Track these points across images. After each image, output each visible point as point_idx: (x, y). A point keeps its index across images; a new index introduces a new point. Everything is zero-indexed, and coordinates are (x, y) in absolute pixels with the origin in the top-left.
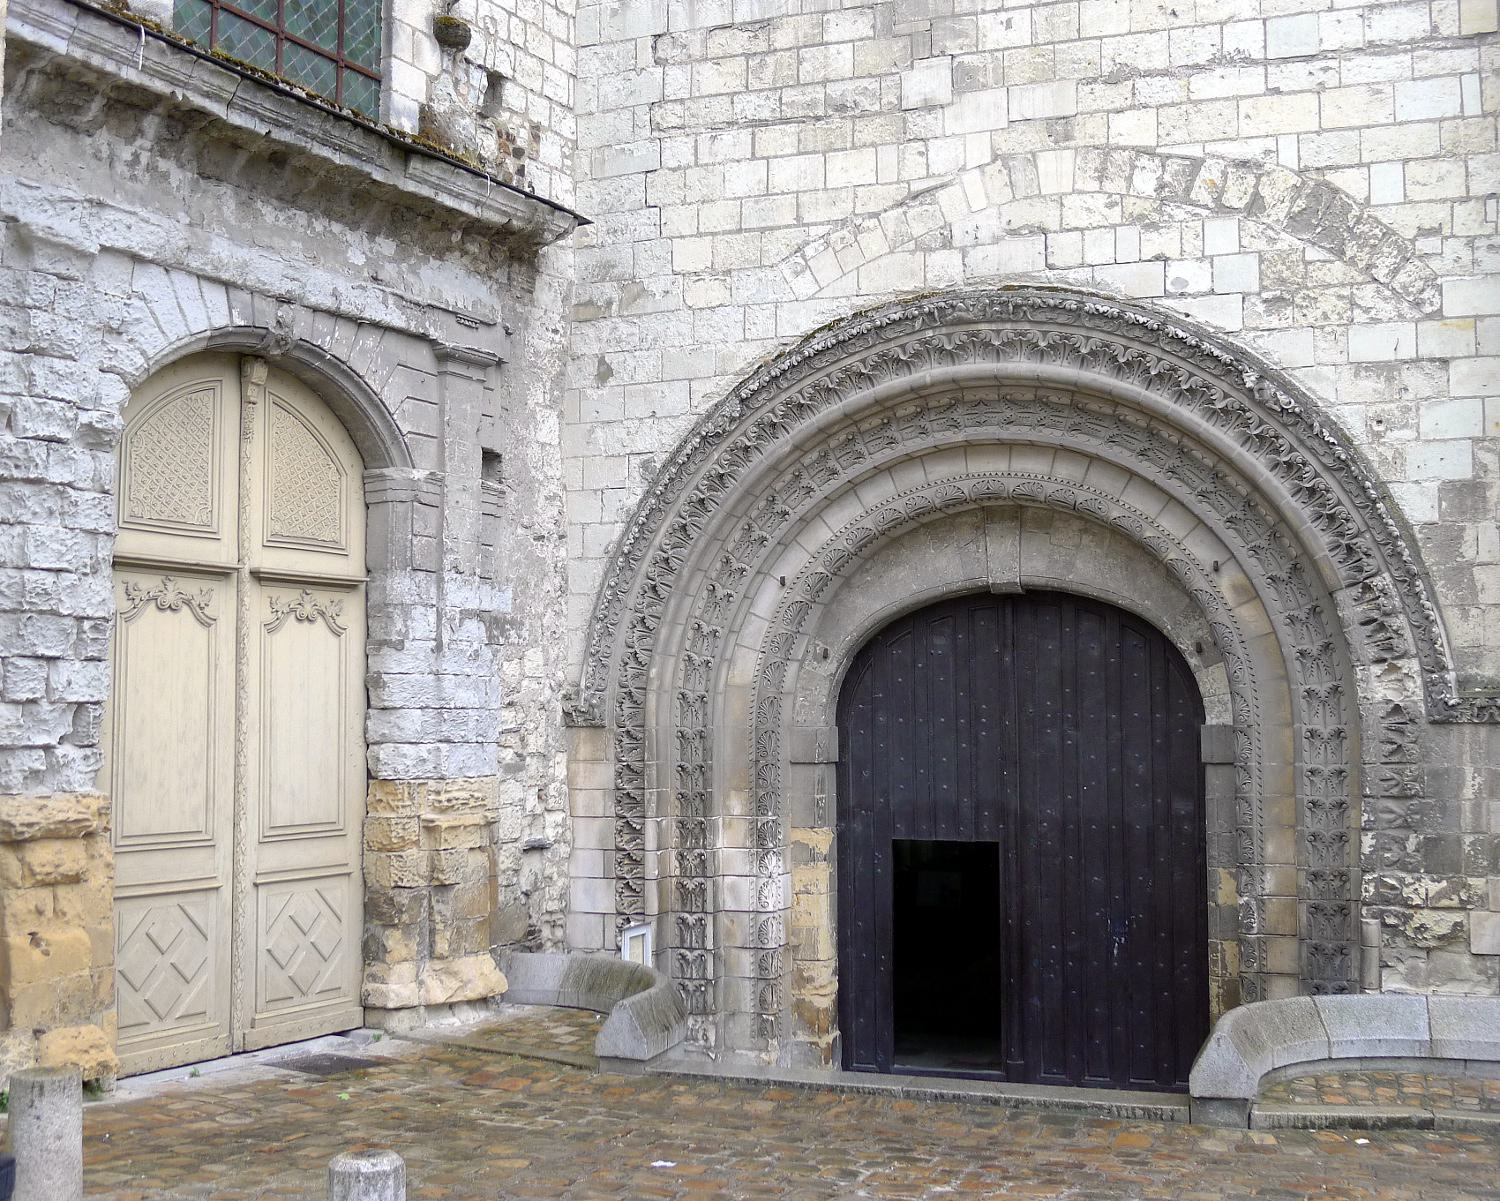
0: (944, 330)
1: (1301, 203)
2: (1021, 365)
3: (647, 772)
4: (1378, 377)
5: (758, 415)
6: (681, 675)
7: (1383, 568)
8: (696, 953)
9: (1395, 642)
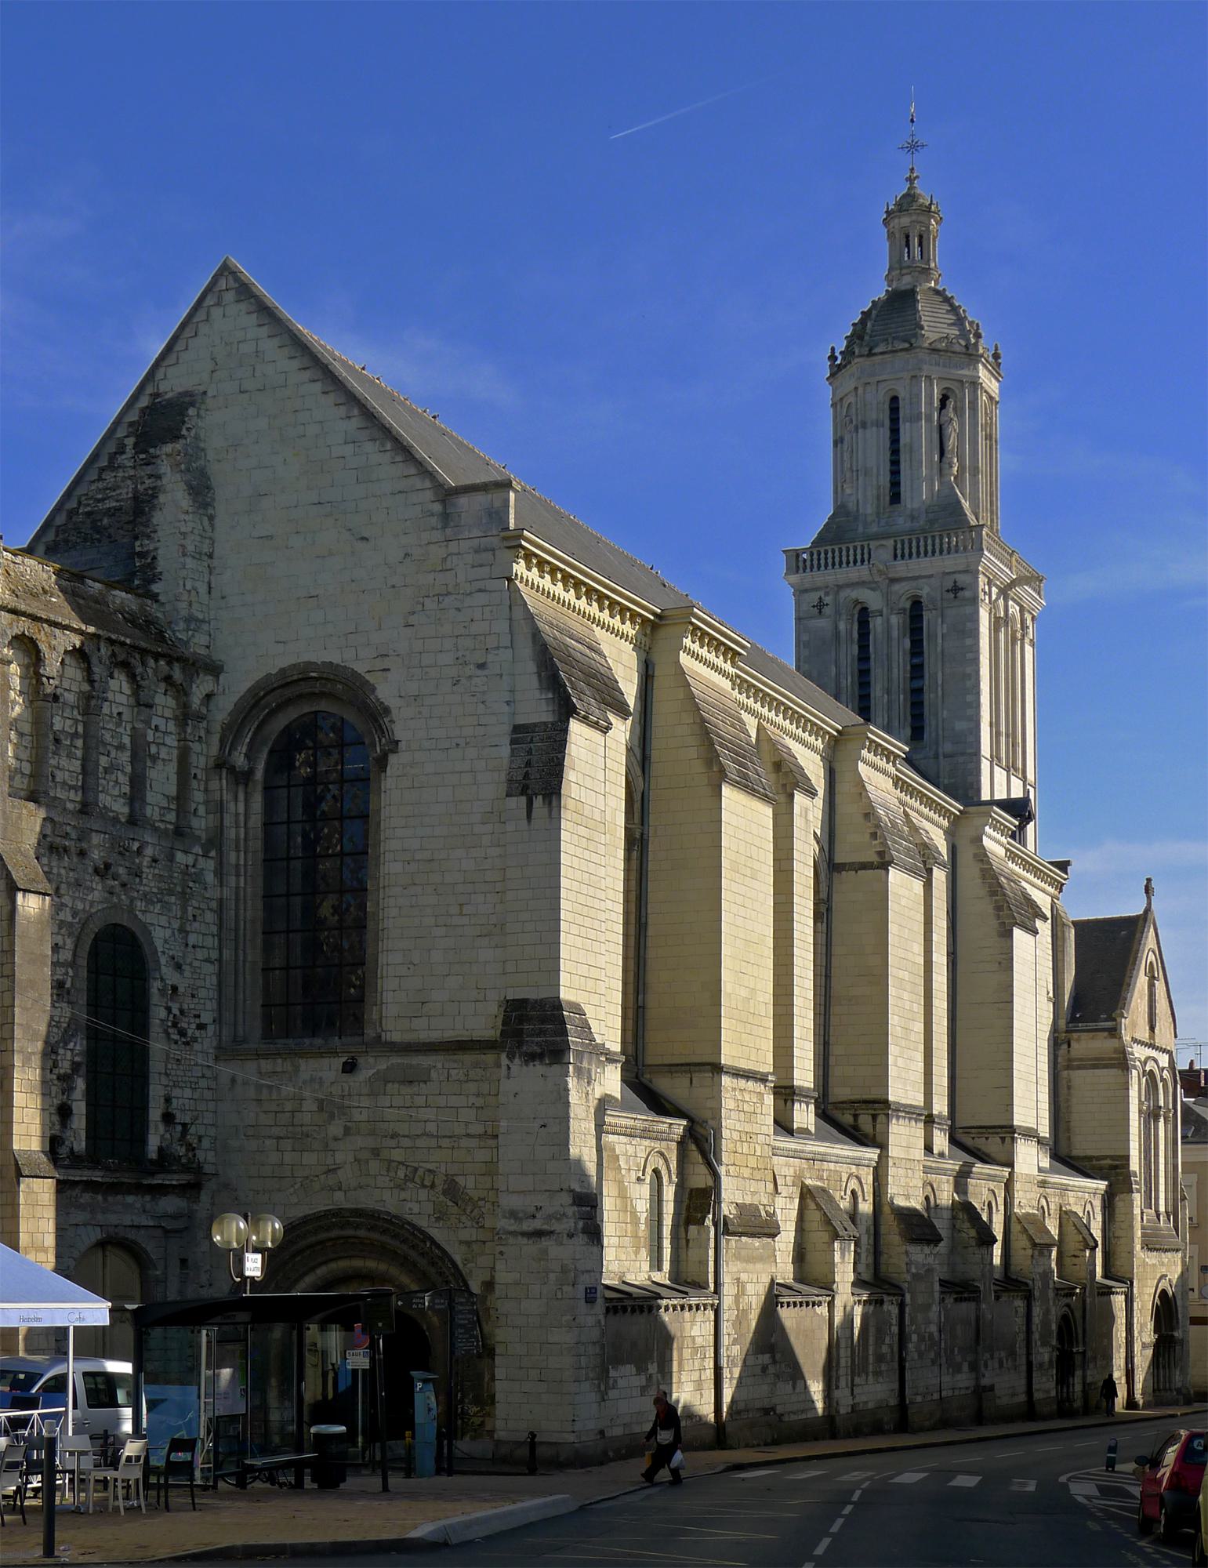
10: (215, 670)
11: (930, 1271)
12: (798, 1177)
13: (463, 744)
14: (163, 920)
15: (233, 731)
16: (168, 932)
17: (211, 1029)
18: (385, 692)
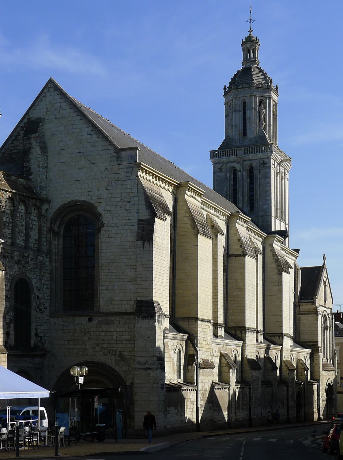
10: (49, 202)
11: (258, 378)
12: (219, 350)
13: (123, 225)
14: (35, 277)
15: (54, 220)
16: (36, 280)
17: (48, 308)
18: (100, 209)
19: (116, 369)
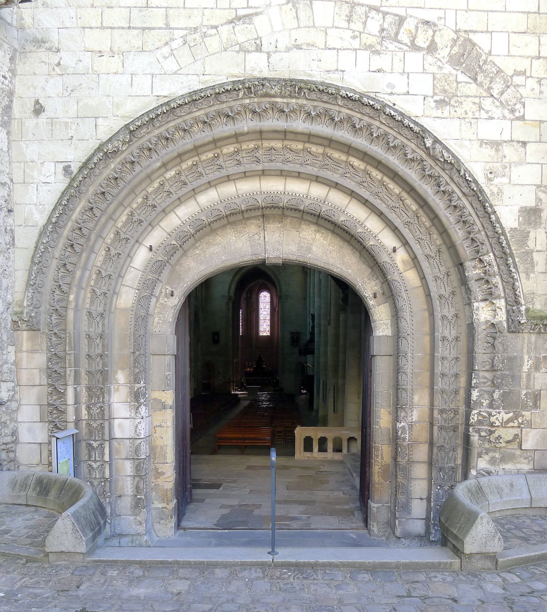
0: (256, 100)
1: (456, 49)
2: (300, 125)
3: (68, 357)
4: (492, 148)
5: (140, 142)
6: (88, 301)
7: (490, 250)
8: (98, 464)
9: (493, 290)
19: (444, 128)
